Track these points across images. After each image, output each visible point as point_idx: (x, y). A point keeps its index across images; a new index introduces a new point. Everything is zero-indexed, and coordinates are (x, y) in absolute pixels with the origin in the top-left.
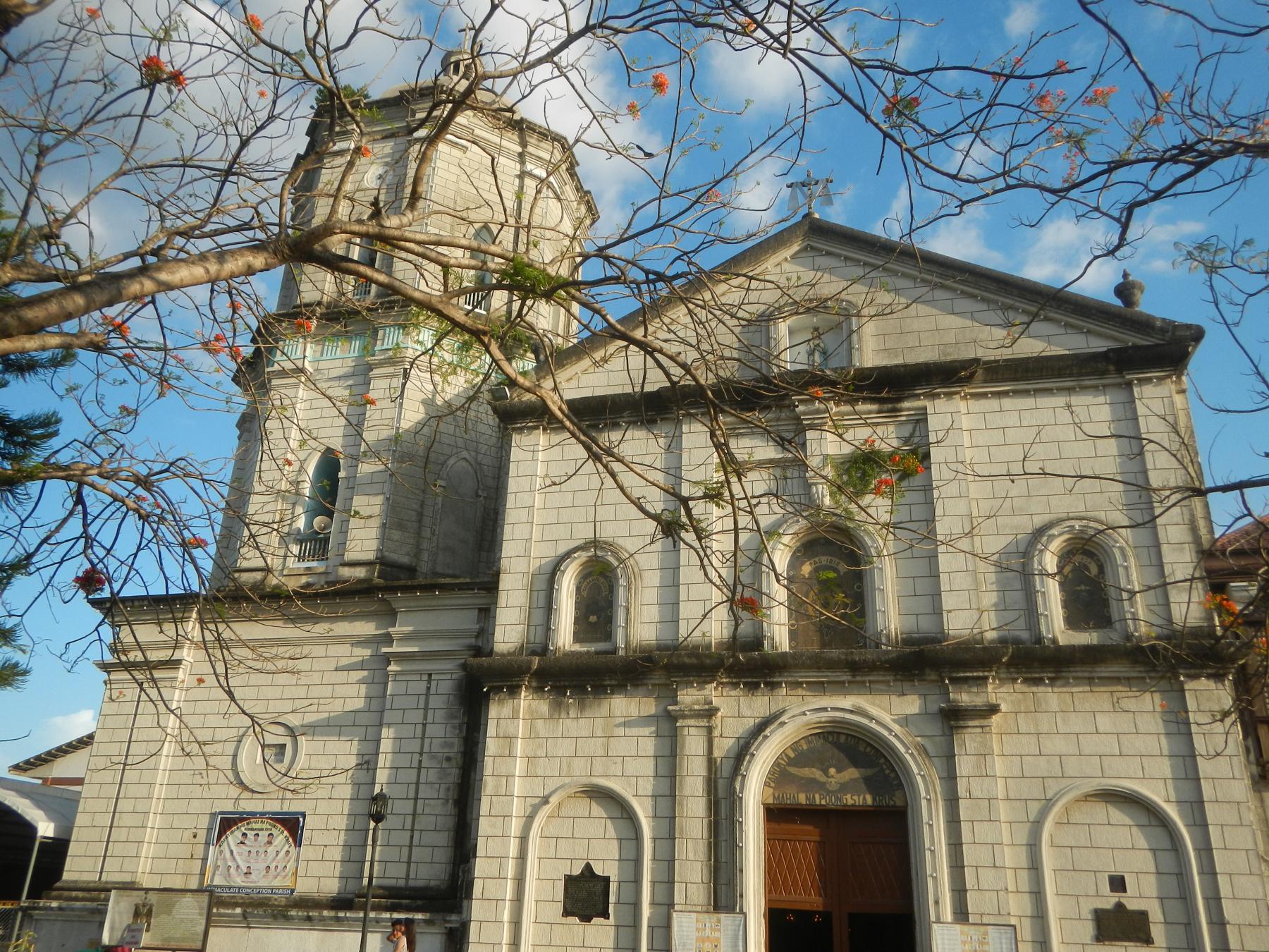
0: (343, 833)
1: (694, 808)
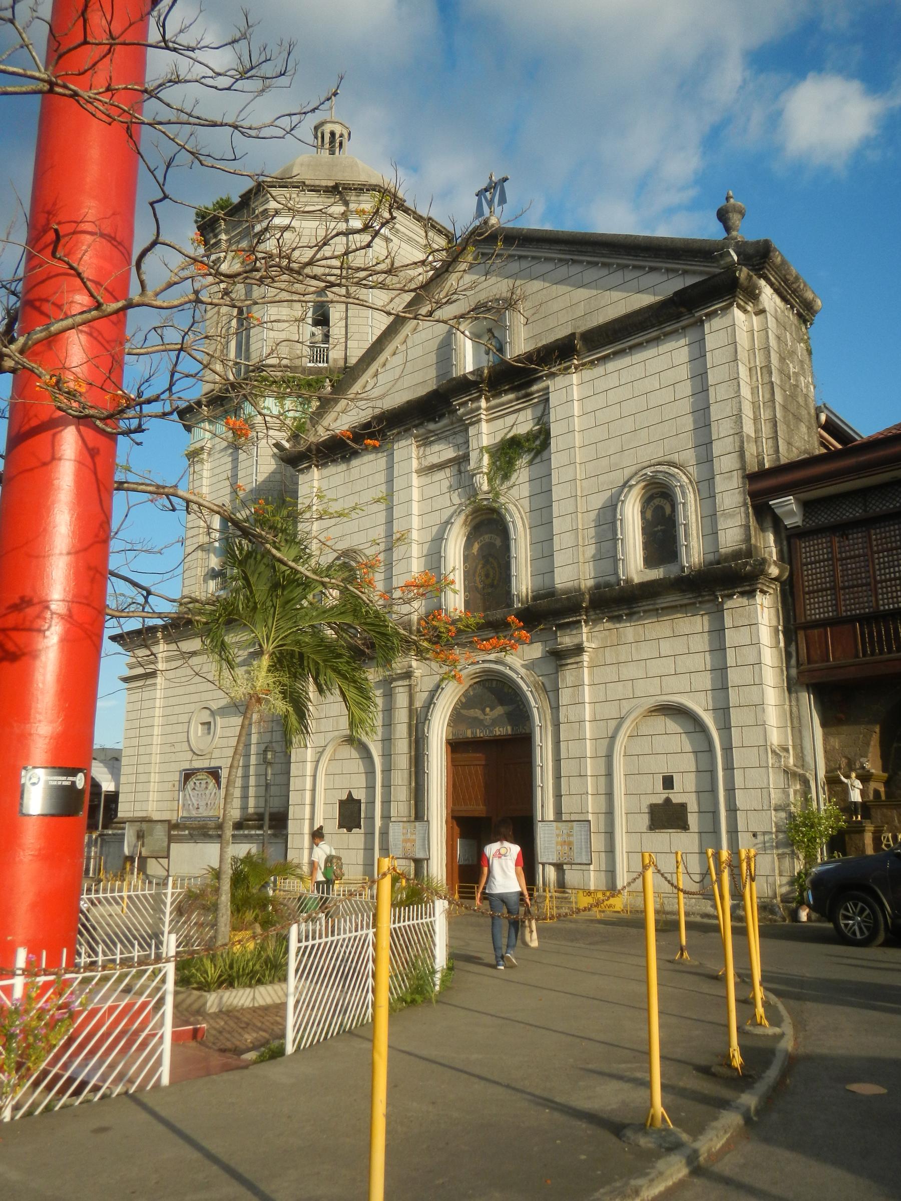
1: (402, 746)
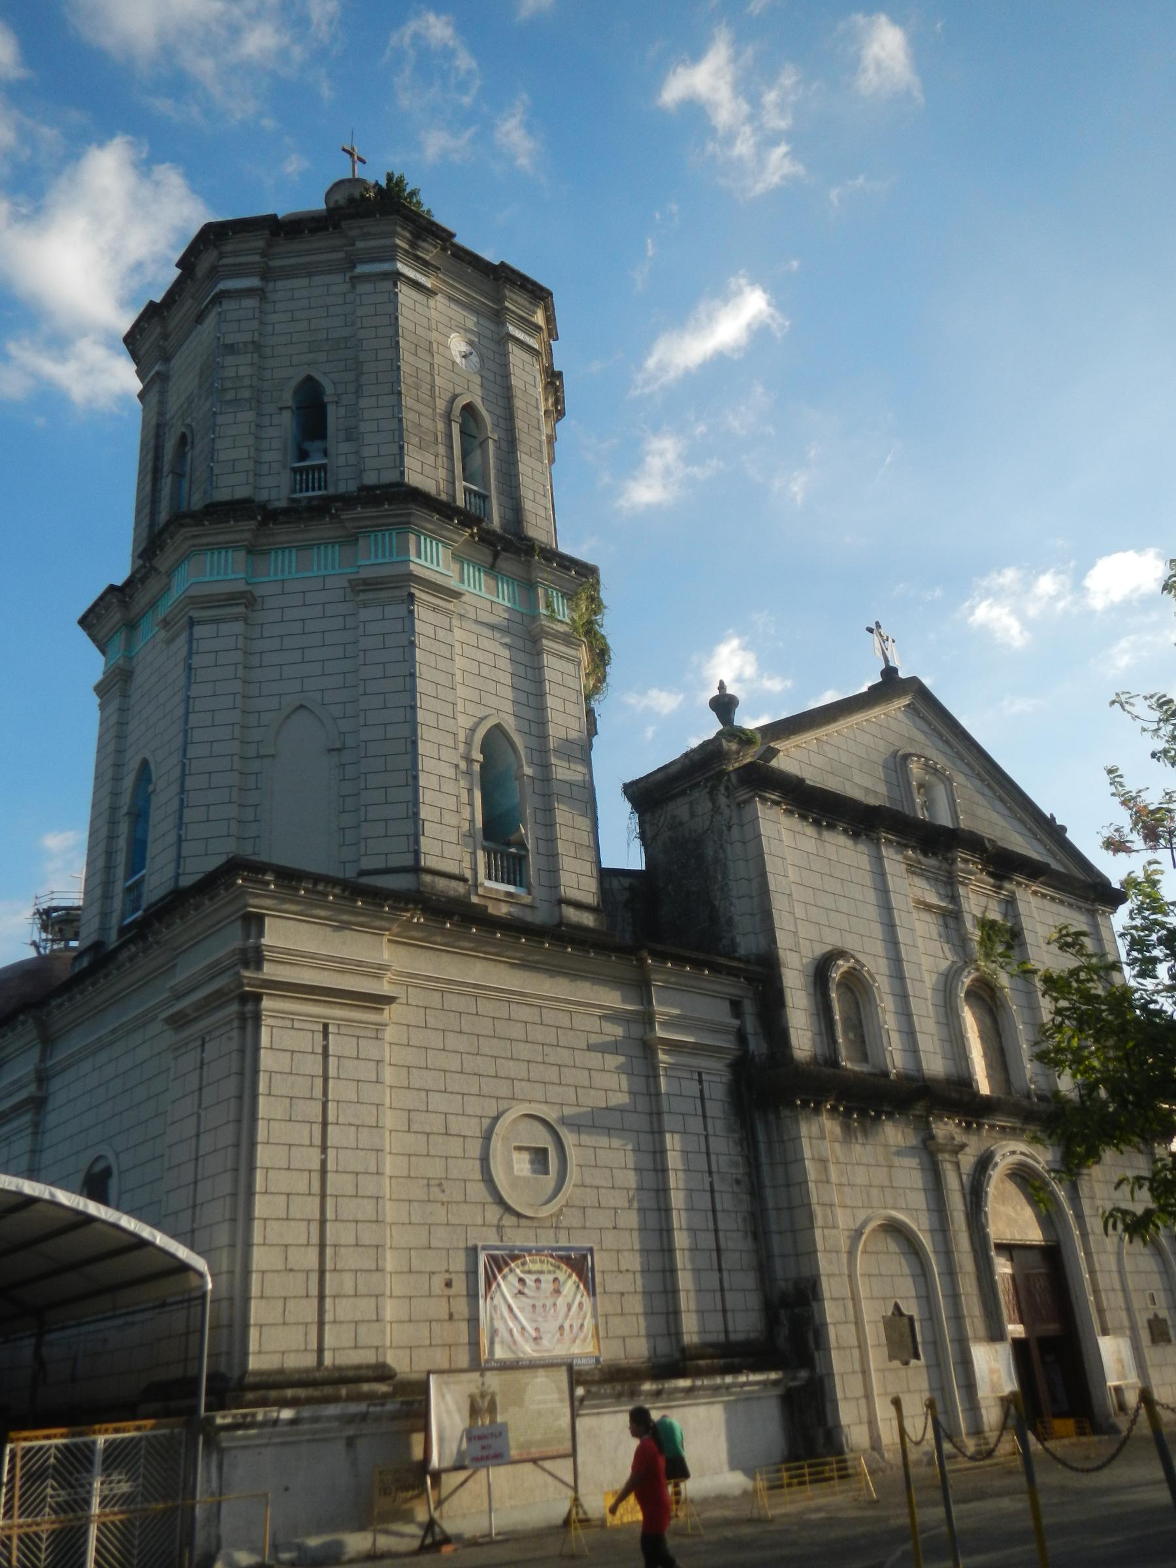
0: (638, 1276)
